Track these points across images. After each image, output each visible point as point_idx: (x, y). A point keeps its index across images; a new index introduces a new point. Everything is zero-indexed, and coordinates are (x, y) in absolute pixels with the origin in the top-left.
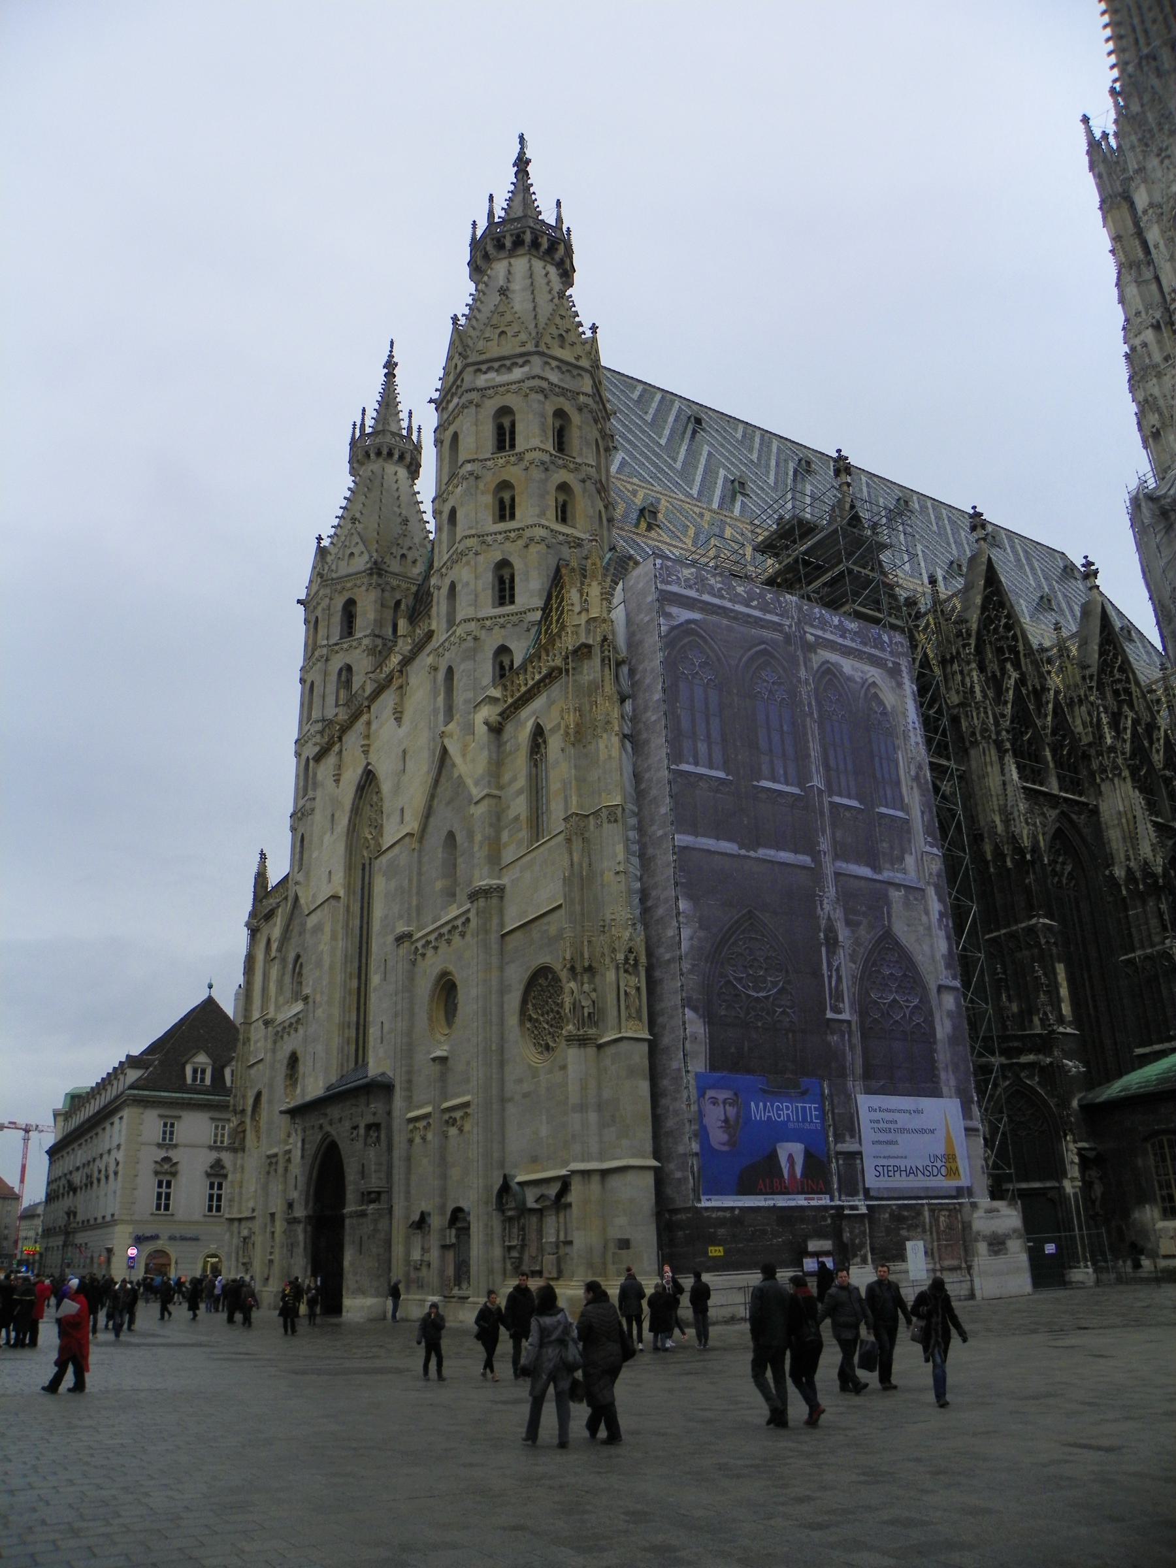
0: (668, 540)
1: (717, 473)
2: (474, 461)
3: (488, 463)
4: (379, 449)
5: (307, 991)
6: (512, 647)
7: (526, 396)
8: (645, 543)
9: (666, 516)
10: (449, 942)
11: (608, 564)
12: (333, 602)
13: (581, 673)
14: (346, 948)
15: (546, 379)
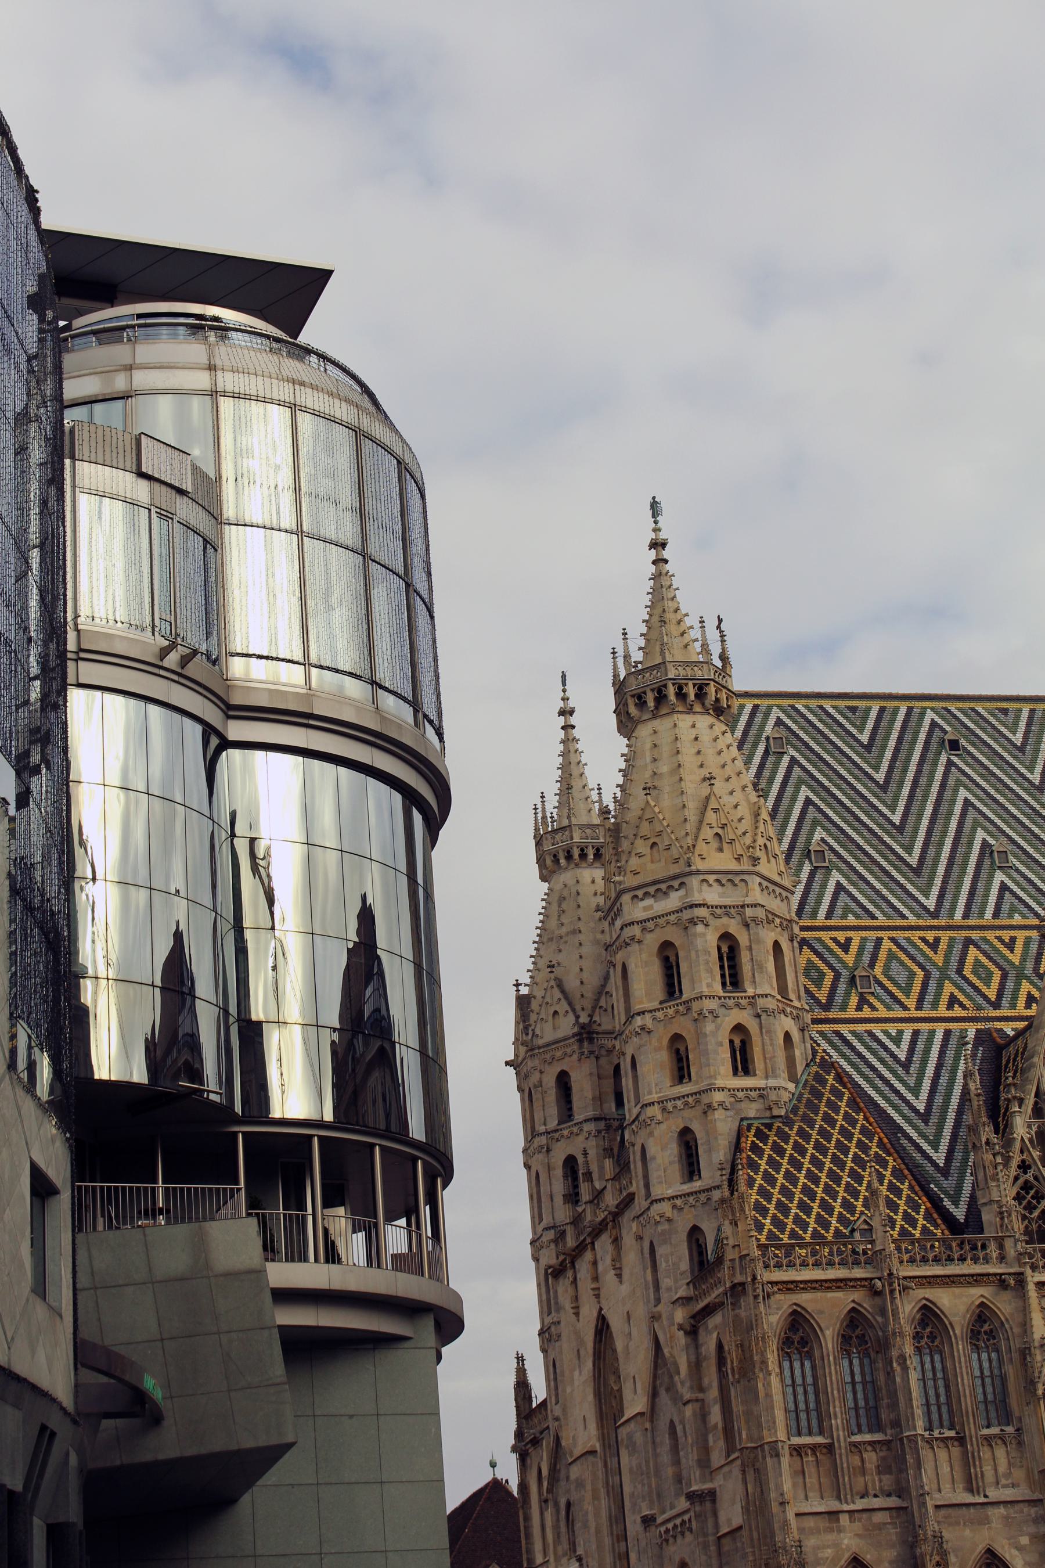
0: (883, 1013)
1: (970, 844)
2: (643, 1013)
3: (659, 1015)
4: (568, 852)
5: (580, 1551)
6: (703, 1228)
7: (687, 928)
8: (853, 1033)
9: (883, 973)
10: (683, 1534)
11: (801, 1095)
12: (544, 1076)
13: (741, 1308)
14: (610, 1507)
15: (704, 905)
